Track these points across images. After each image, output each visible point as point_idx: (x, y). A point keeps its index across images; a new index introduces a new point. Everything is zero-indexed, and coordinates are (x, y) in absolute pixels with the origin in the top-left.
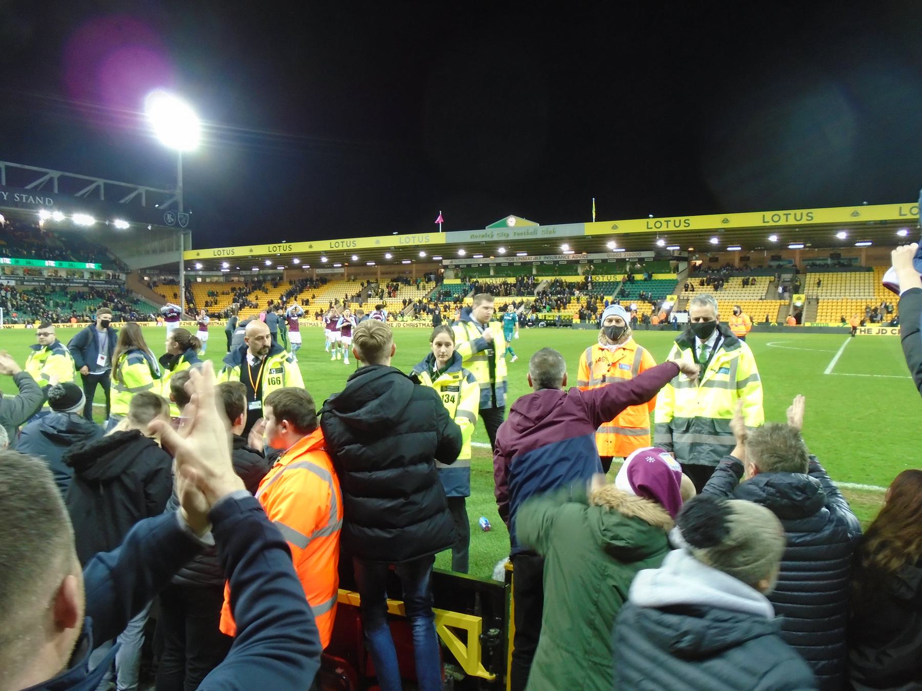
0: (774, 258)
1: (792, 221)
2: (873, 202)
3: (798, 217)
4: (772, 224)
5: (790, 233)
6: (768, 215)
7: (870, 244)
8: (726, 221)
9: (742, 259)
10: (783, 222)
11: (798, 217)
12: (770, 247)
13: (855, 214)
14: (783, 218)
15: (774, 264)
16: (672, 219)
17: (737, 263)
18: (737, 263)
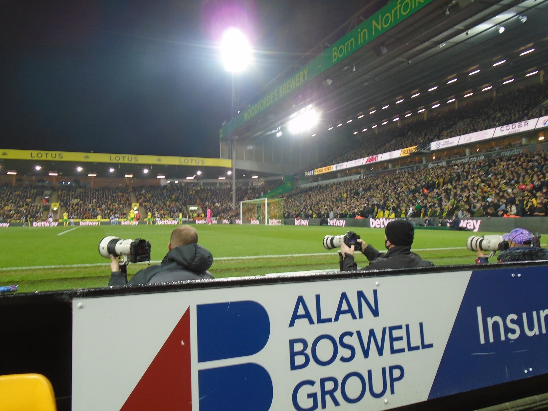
0: (39, 181)
1: (49, 158)
2: (97, 151)
3: (54, 156)
4: (36, 158)
5: (48, 166)
6: (35, 153)
7: (95, 175)
8: (87, 157)
9: (17, 180)
10: (44, 158)
11: (54, 156)
12: (37, 173)
13: (159, 160)
14: (44, 156)
15: (40, 184)
16: (50, 152)
17: (14, 183)
18: (14, 183)
